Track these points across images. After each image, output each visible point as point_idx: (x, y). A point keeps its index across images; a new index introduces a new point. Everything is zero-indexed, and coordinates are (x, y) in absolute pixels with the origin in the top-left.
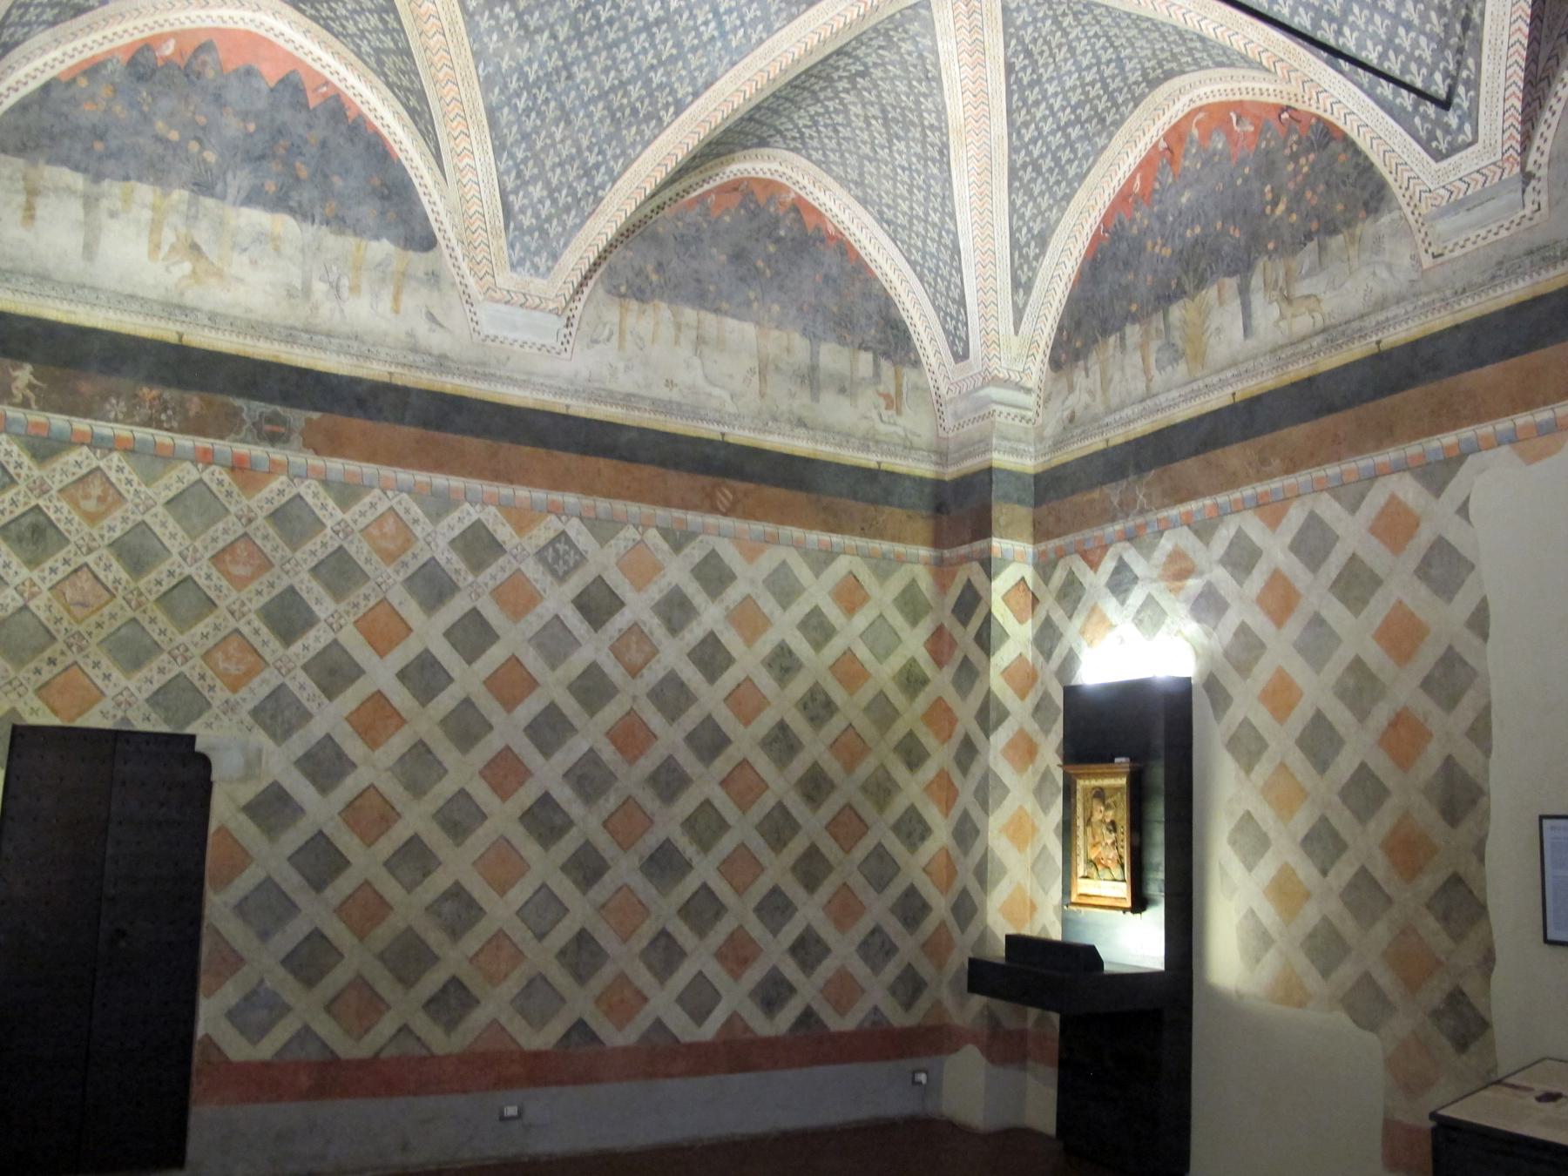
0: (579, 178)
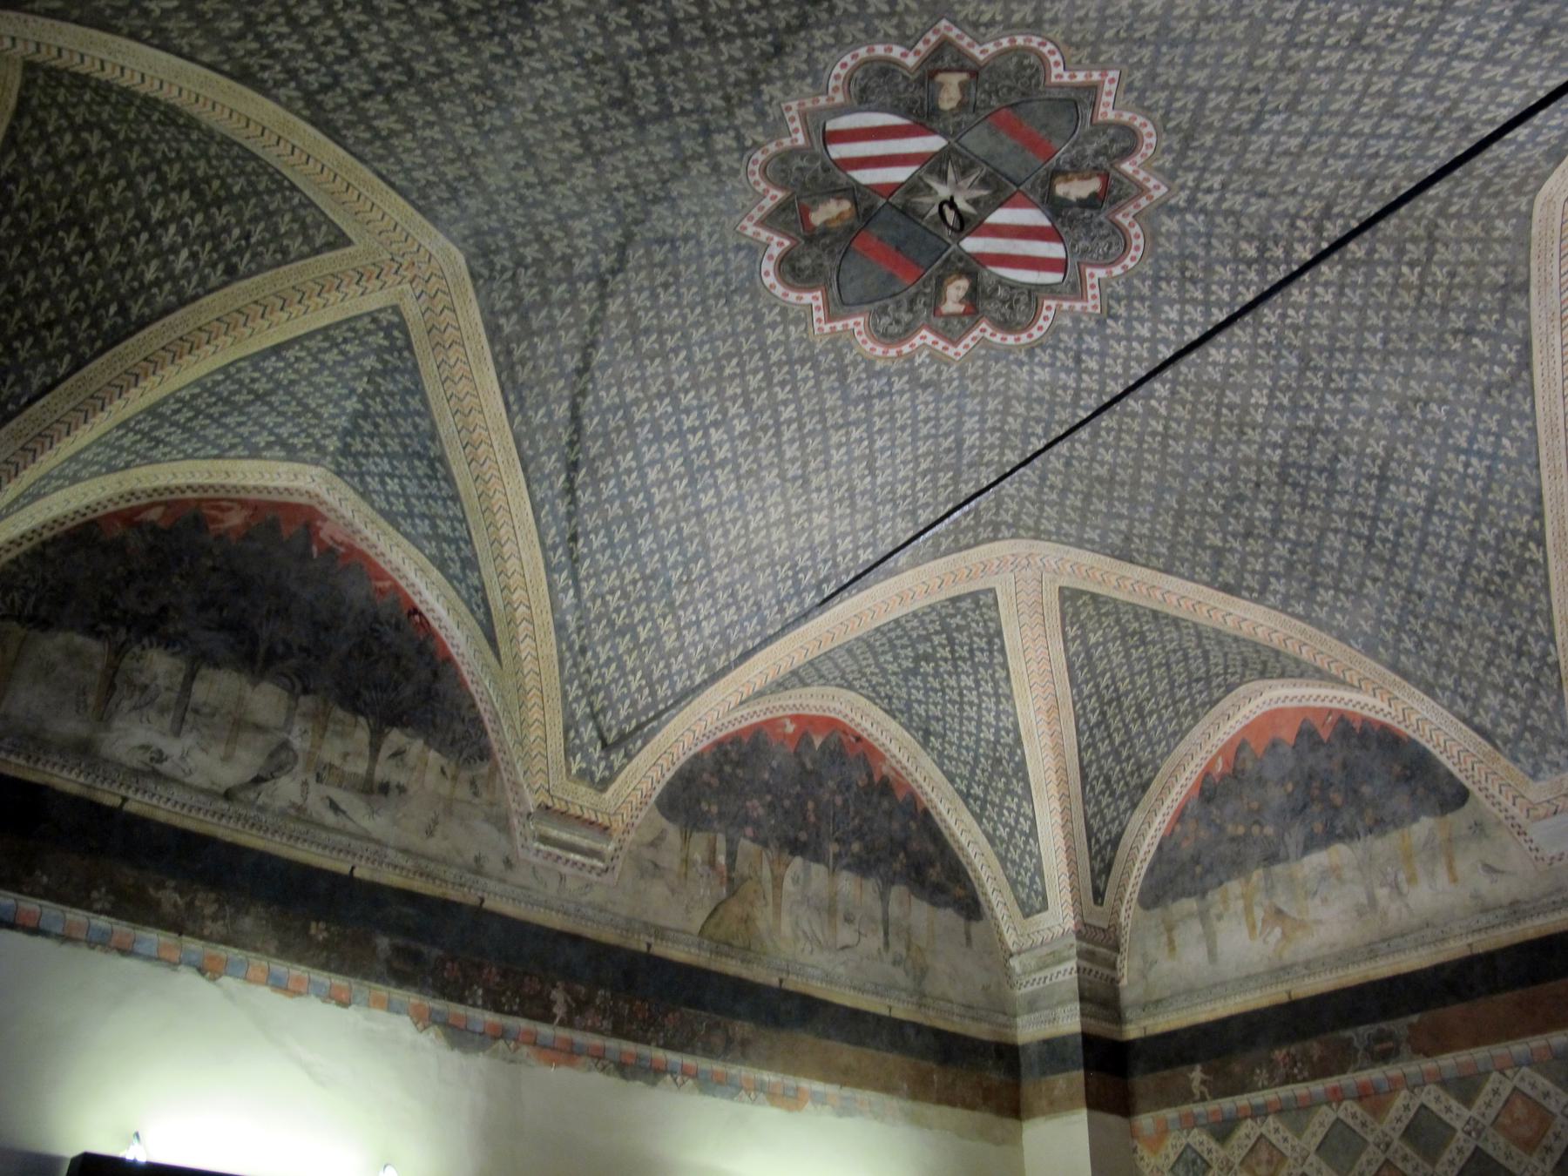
0: (1517, 661)
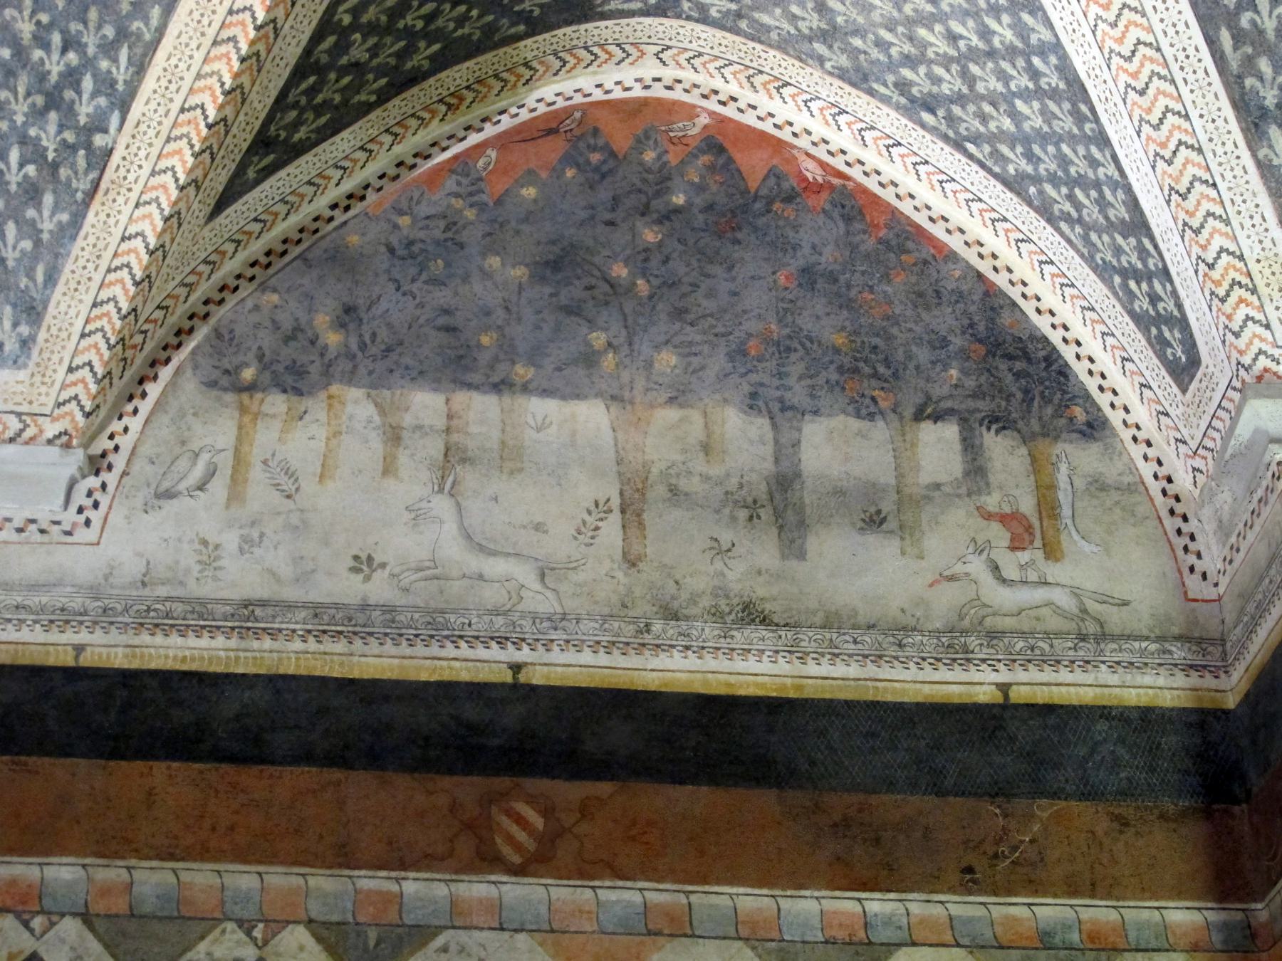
0: (38, 114)
